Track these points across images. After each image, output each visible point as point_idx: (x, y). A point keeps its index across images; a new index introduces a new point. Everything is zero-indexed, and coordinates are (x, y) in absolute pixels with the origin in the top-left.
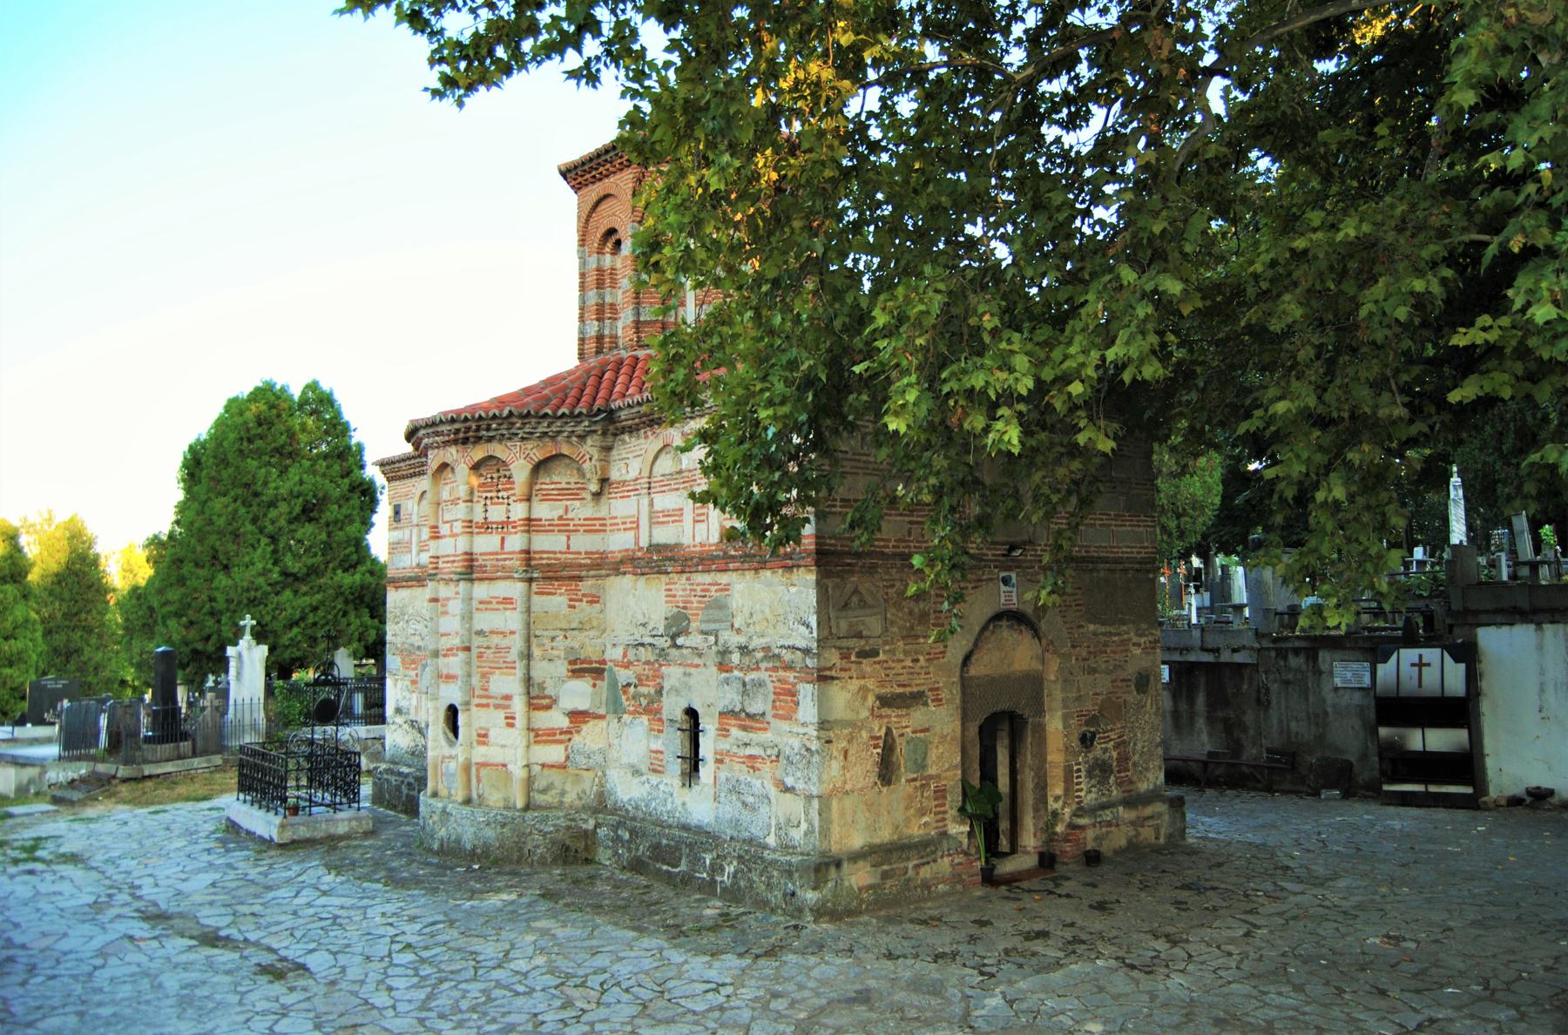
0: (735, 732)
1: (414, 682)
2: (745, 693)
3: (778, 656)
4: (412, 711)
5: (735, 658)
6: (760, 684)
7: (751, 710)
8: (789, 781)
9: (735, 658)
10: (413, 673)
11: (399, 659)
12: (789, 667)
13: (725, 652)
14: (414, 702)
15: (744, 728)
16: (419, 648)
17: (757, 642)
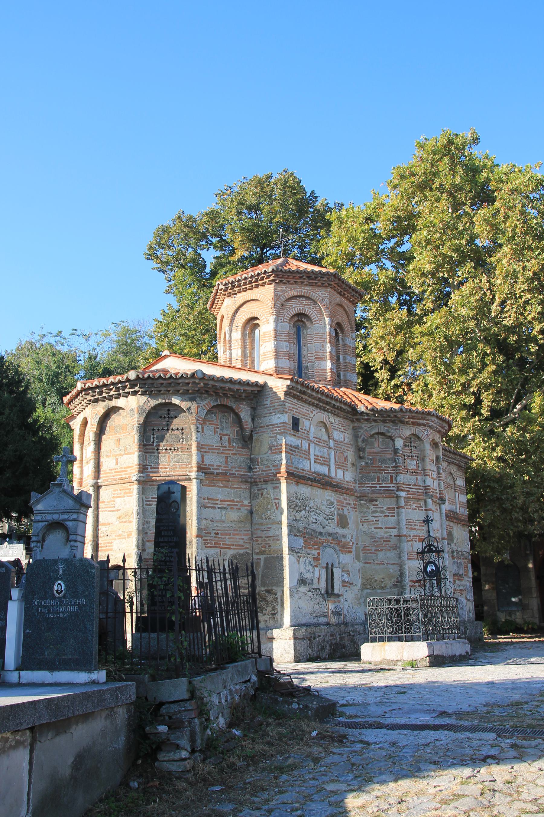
0: (457, 581)
1: (316, 559)
2: (458, 567)
3: (463, 555)
4: (315, 581)
5: (455, 554)
6: (461, 564)
7: (460, 573)
8: (468, 597)
9: (455, 554)
10: (315, 552)
11: (301, 540)
12: (466, 559)
13: (453, 552)
14: (317, 574)
15: (459, 580)
16: (321, 533)
17: (459, 549)
